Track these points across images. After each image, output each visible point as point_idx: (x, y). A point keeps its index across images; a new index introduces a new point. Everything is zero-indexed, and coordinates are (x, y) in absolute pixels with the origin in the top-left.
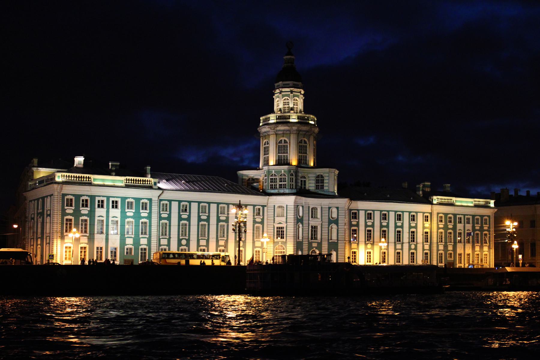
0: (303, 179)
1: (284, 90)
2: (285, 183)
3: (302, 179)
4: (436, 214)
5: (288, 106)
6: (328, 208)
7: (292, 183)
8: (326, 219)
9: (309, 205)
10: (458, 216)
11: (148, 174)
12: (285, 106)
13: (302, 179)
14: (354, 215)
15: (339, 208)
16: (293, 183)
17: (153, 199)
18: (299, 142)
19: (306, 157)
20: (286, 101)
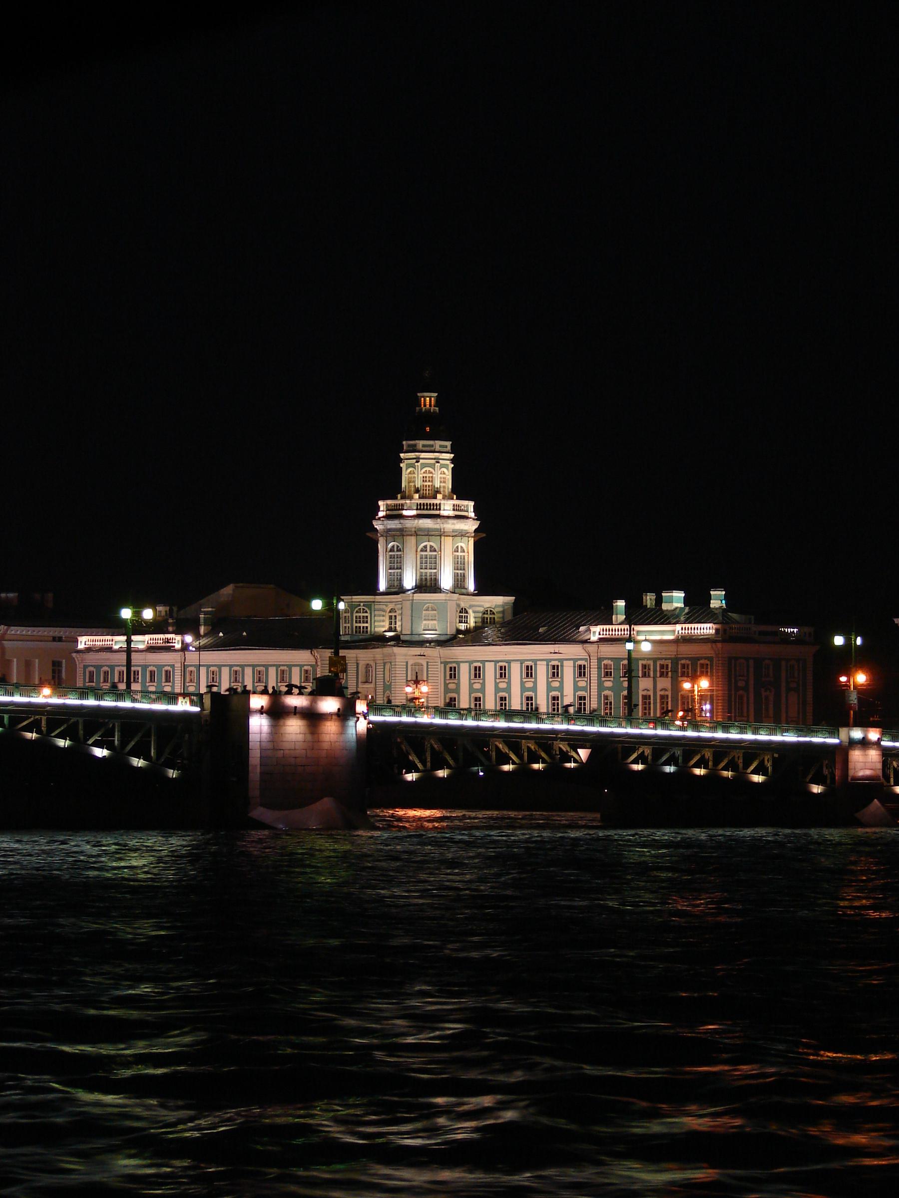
0: (393, 614)
1: (423, 455)
2: (345, 625)
3: (390, 614)
4: (596, 661)
5: (430, 484)
6: (383, 664)
7: (347, 625)
8: (380, 683)
9: (358, 662)
10: (641, 662)
11: (201, 625)
12: (425, 484)
13: (390, 614)
14: (453, 673)
15: (392, 664)
16: (345, 625)
17: (175, 666)
18: (388, 549)
19: (401, 575)
20: (428, 475)
